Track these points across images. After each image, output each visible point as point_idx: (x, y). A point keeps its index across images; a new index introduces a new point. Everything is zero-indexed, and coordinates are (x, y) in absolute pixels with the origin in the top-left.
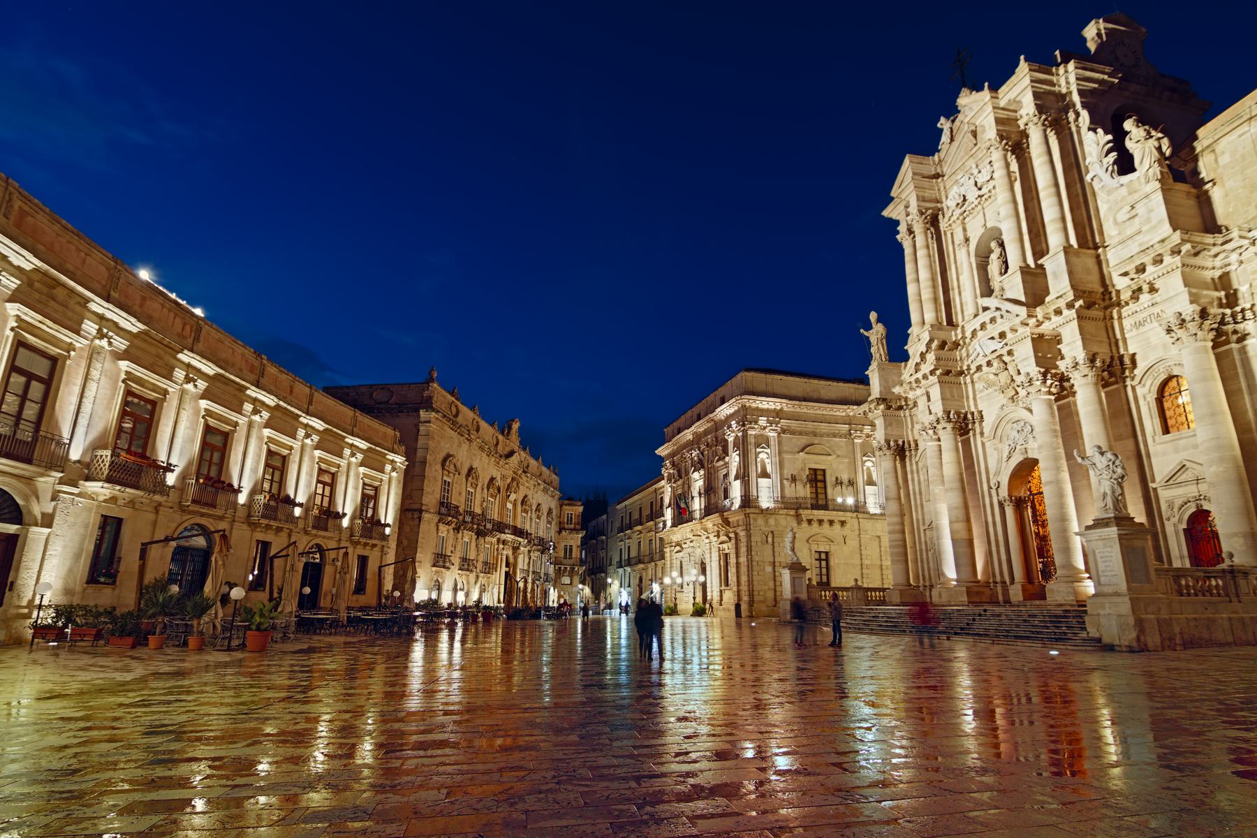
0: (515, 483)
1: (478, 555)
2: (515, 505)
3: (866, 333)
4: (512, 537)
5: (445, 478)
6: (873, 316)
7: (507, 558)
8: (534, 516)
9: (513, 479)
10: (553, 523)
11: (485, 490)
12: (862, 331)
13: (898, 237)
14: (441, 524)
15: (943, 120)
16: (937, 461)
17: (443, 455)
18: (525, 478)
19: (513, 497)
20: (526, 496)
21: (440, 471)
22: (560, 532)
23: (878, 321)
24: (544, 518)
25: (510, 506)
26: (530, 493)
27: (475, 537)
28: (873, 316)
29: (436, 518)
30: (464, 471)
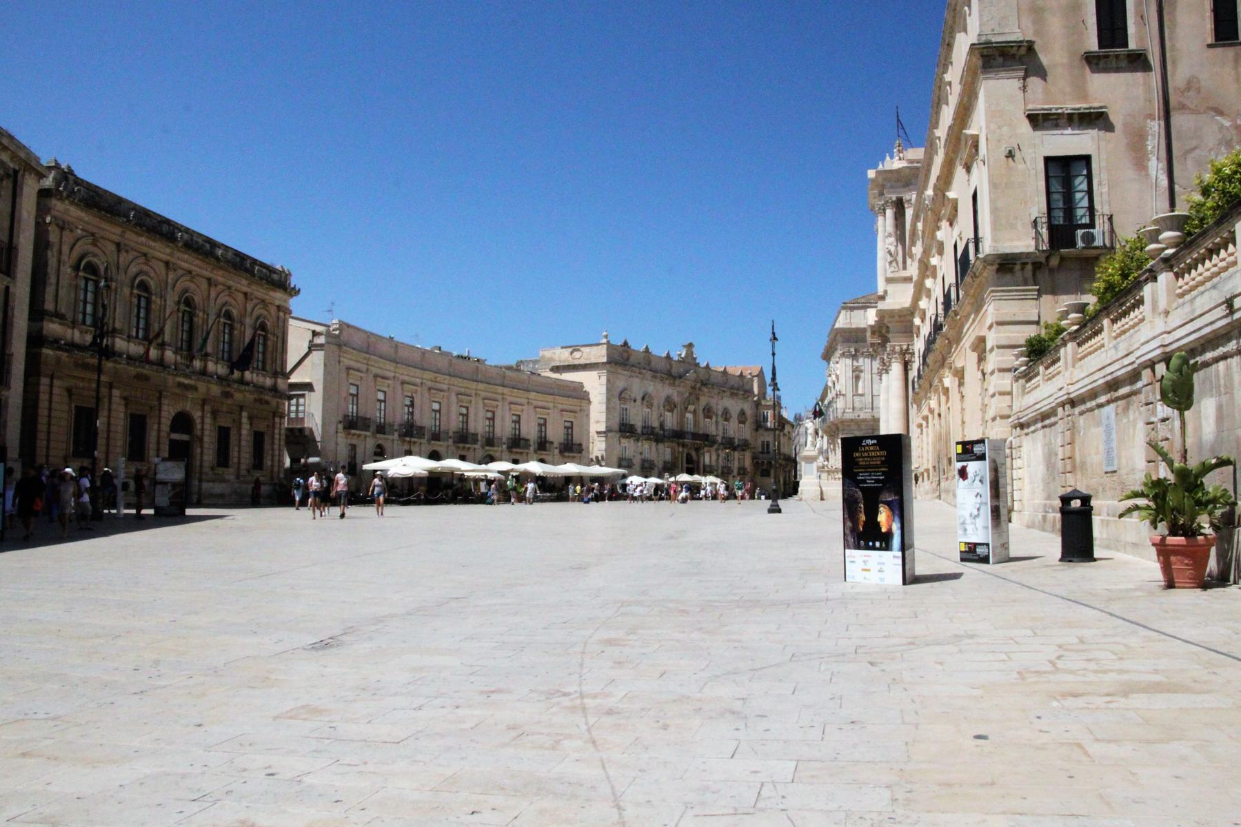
2: (694, 412)
5: (622, 406)
7: (689, 456)
8: (720, 419)
11: (662, 408)
17: (619, 390)
18: (705, 390)
19: (691, 408)
20: (707, 404)
21: (618, 402)
22: (757, 430)
25: (689, 416)
26: (713, 402)
29: (618, 435)
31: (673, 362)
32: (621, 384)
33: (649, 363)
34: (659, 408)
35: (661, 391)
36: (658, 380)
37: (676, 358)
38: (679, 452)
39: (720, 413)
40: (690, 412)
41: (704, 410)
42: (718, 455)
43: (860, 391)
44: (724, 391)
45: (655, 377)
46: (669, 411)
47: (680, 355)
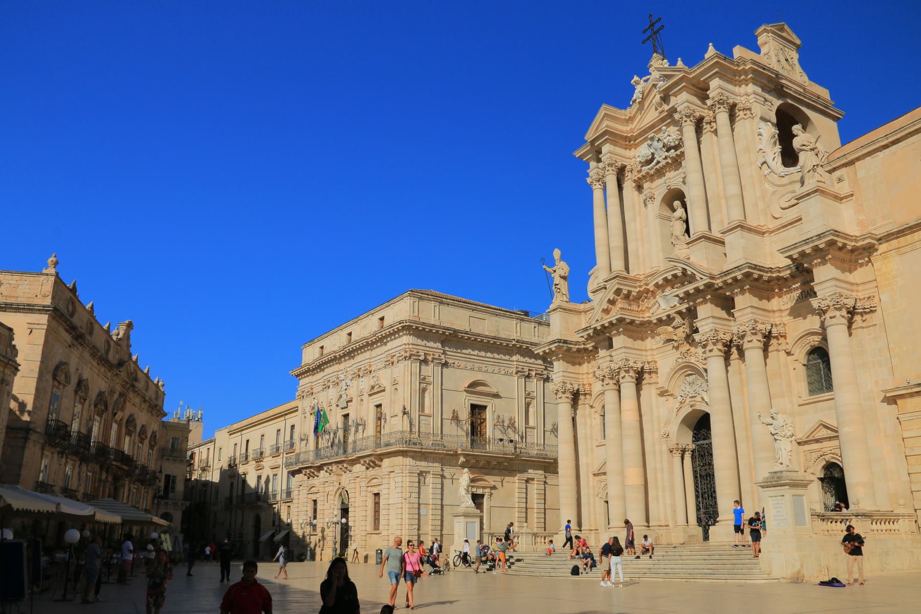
0: (122, 399)
1: (79, 485)
2: (120, 425)
3: (548, 269)
4: (118, 464)
6: (557, 253)
8: (137, 439)
9: (121, 395)
10: (155, 448)
11: (92, 407)
12: (544, 267)
13: (589, 180)
14: (47, 447)
15: (636, 78)
16: (616, 406)
17: (56, 362)
19: (119, 415)
20: (131, 415)
21: (51, 382)
23: (562, 258)
24: (147, 442)
27: (78, 464)
28: (557, 253)
30: (74, 381)
31: (112, 344)
32: (60, 354)
33: (91, 333)
34: (90, 405)
35: (98, 382)
36: (95, 363)
37: (115, 338)
38: (100, 480)
39: (138, 429)
40: (116, 422)
41: (127, 422)
42: (129, 490)
43: (427, 411)
44: (145, 401)
45: (93, 355)
46: (98, 415)
47: (118, 334)
